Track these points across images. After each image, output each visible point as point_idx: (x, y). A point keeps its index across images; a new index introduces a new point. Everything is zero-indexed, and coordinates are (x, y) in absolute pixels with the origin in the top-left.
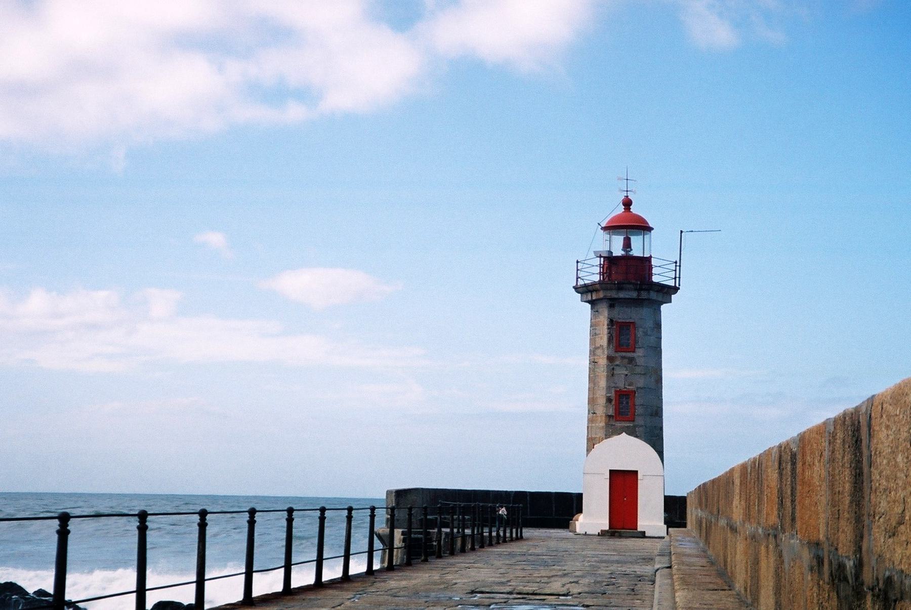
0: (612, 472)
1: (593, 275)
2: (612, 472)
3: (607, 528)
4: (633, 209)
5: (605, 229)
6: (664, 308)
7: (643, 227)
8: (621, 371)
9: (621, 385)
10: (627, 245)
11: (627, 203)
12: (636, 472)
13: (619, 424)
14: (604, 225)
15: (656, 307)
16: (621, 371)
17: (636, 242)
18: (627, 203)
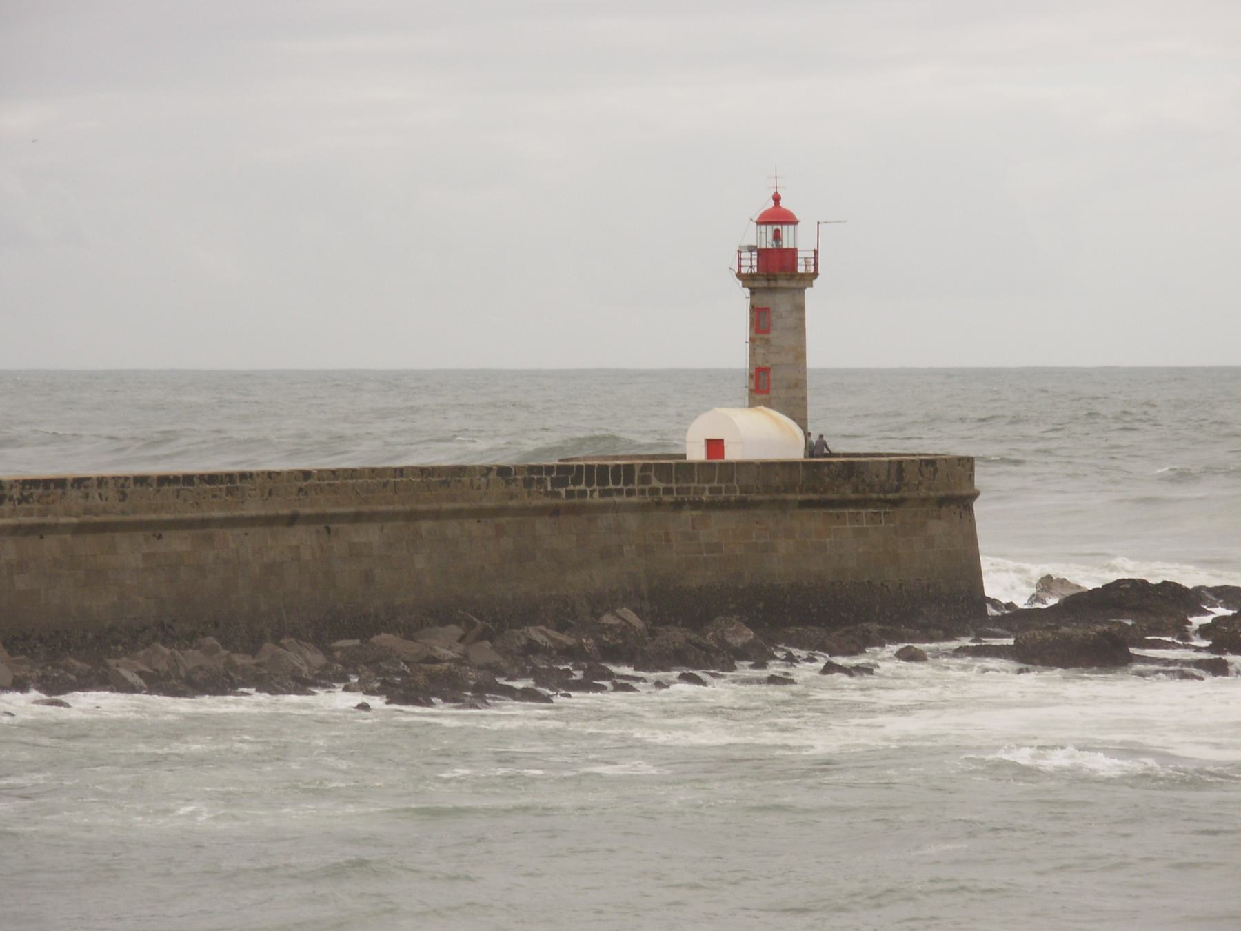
4: (782, 204)
5: (759, 223)
7: (790, 220)
8: (760, 351)
9: (760, 363)
10: (777, 236)
11: (777, 199)
13: (759, 397)
14: (755, 219)
15: (801, 290)
16: (760, 351)
17: (785, 230)
18: (777, 199)
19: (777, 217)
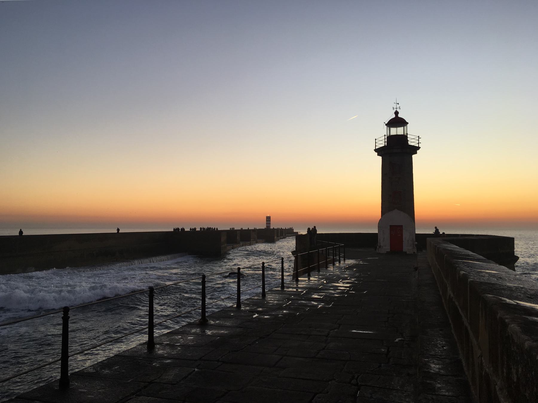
0: (391, 226)
1: (382, 144)
2: (391, 226)
3: (389, 250)
4: (399, 116)
6: (414, 156)
11: (397, 113)
12: (401, 226)
14: (386, 123)
18: (397, 113)
19: (397, 121)
